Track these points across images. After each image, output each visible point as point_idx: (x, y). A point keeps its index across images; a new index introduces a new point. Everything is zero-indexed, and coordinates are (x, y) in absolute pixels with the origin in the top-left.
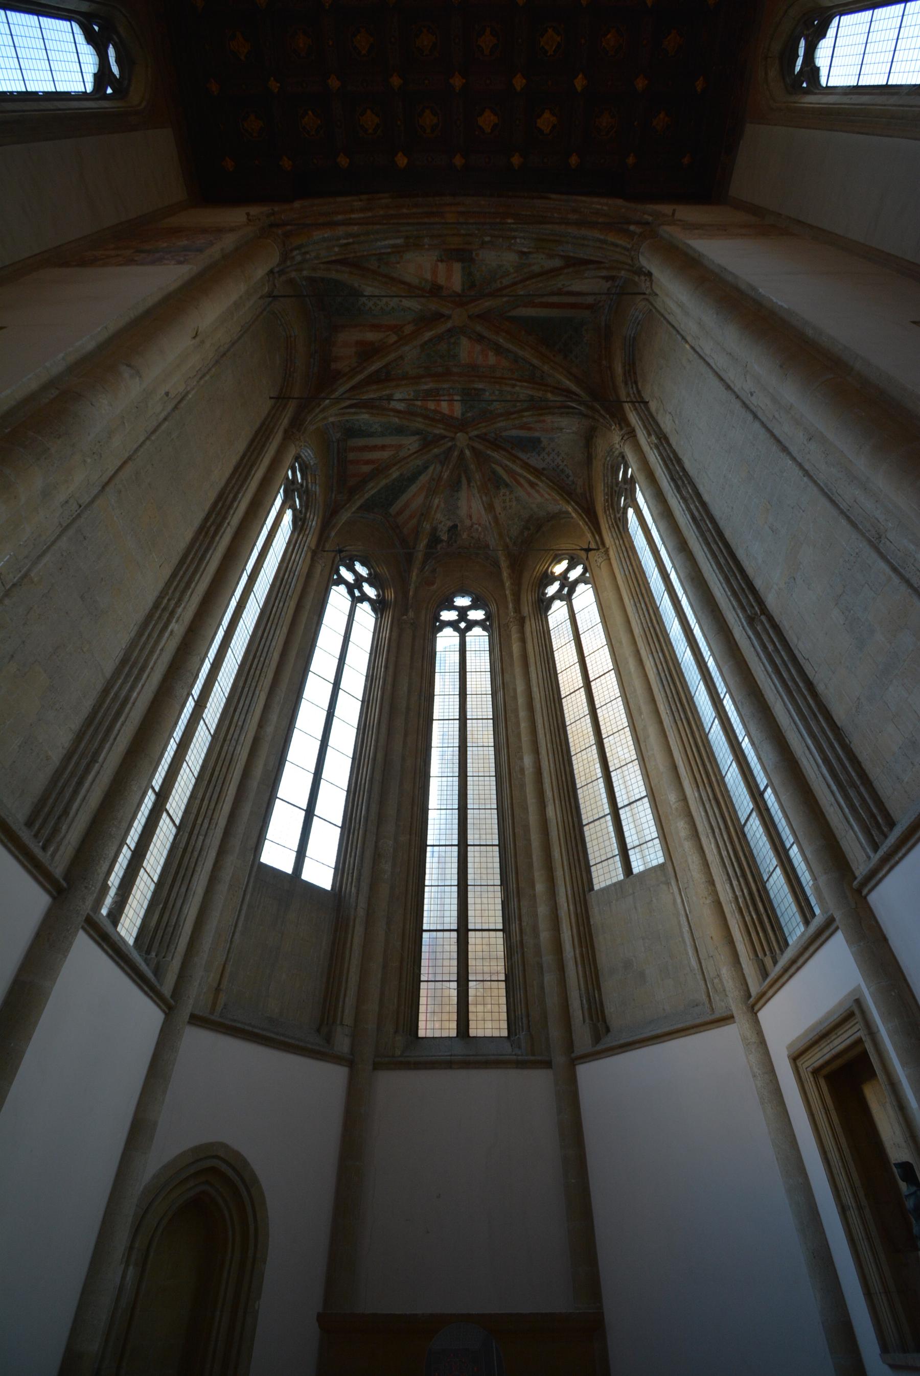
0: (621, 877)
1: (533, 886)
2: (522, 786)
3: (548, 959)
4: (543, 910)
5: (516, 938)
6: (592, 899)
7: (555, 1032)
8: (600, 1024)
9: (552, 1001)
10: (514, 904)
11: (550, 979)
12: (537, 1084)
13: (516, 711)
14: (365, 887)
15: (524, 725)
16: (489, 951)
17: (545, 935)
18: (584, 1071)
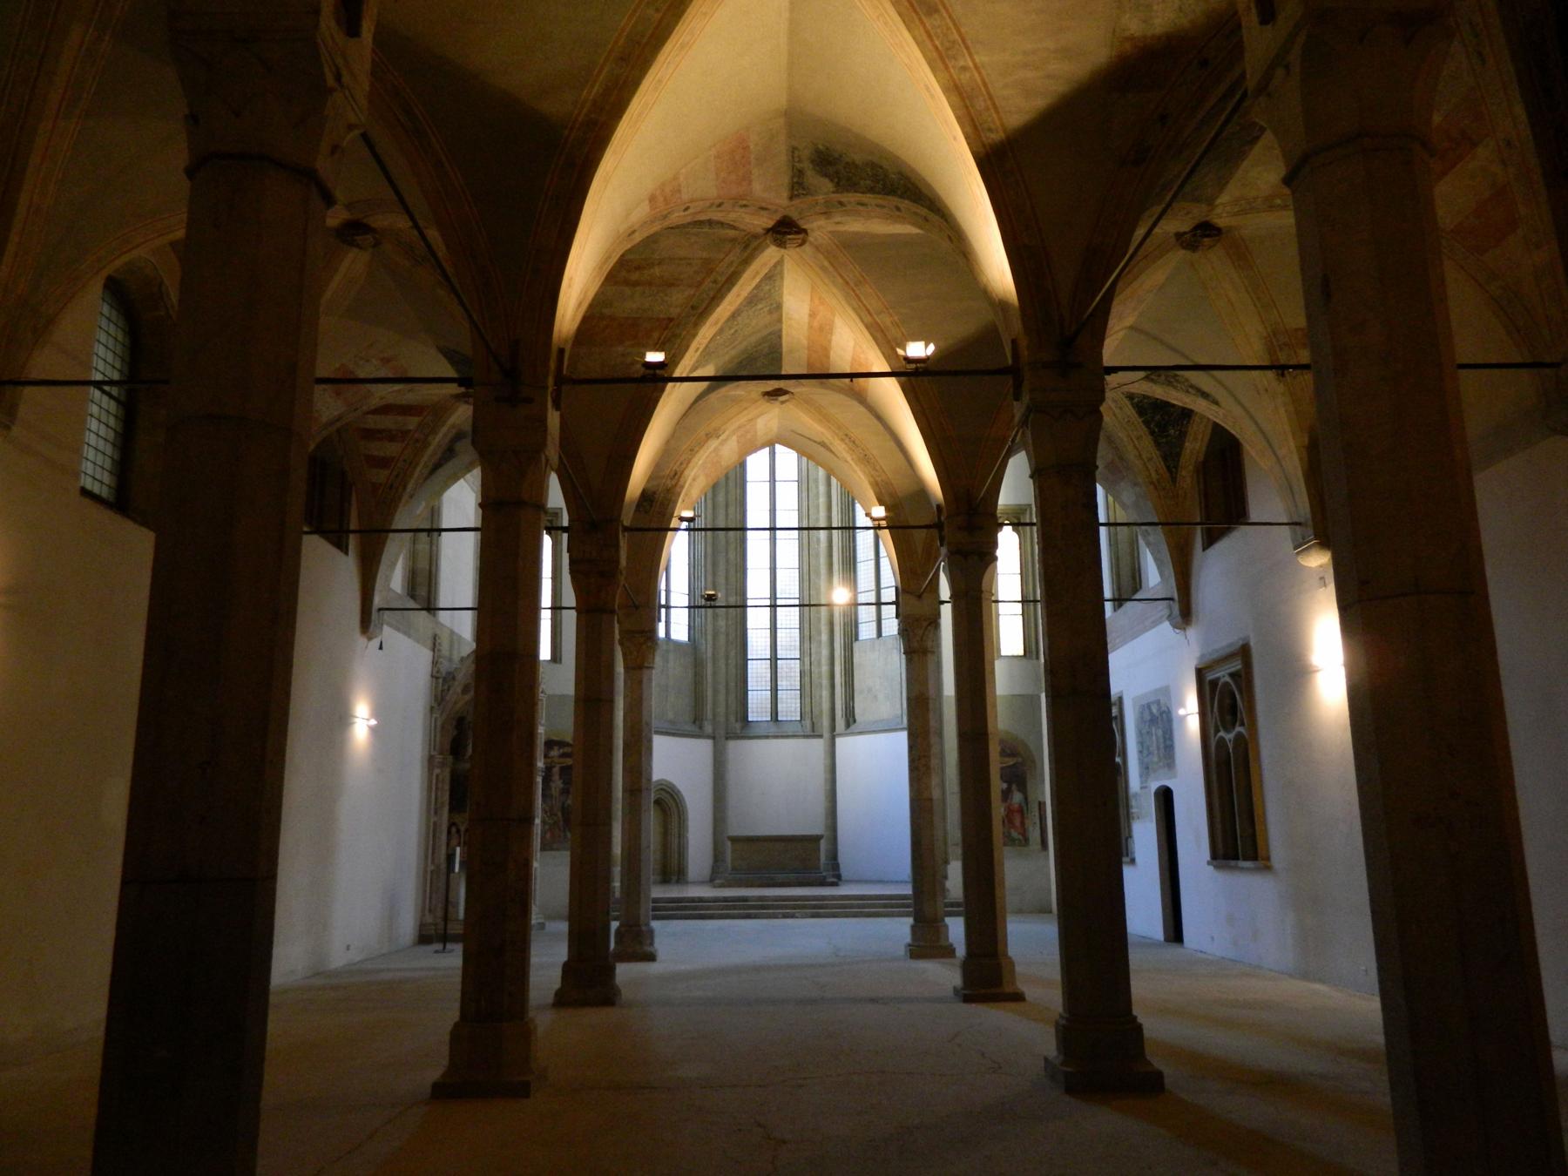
0: (875, 636)
1: (820, 634)
2: (818, 555)
3: (825, 682)
4: (825, 652)
5: (807, 667)
6: (856, 646)
7: (826, 722)
8: (850, 718)
9: (826, 706)
10: (807, 645)
11: (825, 693)
12: (818, 746)
13: (816, 481)
14: (710, 638)
15: (822, 500)
16: (790, 674)
17: (825, 668)
18: (839, 741)
